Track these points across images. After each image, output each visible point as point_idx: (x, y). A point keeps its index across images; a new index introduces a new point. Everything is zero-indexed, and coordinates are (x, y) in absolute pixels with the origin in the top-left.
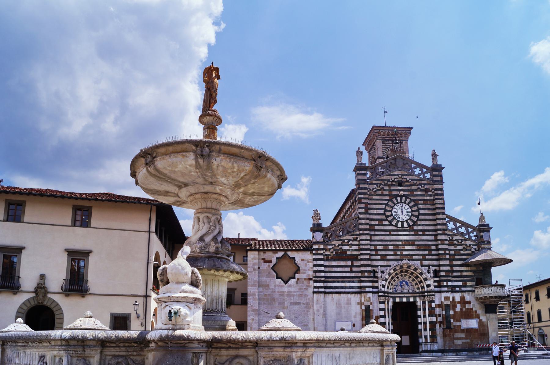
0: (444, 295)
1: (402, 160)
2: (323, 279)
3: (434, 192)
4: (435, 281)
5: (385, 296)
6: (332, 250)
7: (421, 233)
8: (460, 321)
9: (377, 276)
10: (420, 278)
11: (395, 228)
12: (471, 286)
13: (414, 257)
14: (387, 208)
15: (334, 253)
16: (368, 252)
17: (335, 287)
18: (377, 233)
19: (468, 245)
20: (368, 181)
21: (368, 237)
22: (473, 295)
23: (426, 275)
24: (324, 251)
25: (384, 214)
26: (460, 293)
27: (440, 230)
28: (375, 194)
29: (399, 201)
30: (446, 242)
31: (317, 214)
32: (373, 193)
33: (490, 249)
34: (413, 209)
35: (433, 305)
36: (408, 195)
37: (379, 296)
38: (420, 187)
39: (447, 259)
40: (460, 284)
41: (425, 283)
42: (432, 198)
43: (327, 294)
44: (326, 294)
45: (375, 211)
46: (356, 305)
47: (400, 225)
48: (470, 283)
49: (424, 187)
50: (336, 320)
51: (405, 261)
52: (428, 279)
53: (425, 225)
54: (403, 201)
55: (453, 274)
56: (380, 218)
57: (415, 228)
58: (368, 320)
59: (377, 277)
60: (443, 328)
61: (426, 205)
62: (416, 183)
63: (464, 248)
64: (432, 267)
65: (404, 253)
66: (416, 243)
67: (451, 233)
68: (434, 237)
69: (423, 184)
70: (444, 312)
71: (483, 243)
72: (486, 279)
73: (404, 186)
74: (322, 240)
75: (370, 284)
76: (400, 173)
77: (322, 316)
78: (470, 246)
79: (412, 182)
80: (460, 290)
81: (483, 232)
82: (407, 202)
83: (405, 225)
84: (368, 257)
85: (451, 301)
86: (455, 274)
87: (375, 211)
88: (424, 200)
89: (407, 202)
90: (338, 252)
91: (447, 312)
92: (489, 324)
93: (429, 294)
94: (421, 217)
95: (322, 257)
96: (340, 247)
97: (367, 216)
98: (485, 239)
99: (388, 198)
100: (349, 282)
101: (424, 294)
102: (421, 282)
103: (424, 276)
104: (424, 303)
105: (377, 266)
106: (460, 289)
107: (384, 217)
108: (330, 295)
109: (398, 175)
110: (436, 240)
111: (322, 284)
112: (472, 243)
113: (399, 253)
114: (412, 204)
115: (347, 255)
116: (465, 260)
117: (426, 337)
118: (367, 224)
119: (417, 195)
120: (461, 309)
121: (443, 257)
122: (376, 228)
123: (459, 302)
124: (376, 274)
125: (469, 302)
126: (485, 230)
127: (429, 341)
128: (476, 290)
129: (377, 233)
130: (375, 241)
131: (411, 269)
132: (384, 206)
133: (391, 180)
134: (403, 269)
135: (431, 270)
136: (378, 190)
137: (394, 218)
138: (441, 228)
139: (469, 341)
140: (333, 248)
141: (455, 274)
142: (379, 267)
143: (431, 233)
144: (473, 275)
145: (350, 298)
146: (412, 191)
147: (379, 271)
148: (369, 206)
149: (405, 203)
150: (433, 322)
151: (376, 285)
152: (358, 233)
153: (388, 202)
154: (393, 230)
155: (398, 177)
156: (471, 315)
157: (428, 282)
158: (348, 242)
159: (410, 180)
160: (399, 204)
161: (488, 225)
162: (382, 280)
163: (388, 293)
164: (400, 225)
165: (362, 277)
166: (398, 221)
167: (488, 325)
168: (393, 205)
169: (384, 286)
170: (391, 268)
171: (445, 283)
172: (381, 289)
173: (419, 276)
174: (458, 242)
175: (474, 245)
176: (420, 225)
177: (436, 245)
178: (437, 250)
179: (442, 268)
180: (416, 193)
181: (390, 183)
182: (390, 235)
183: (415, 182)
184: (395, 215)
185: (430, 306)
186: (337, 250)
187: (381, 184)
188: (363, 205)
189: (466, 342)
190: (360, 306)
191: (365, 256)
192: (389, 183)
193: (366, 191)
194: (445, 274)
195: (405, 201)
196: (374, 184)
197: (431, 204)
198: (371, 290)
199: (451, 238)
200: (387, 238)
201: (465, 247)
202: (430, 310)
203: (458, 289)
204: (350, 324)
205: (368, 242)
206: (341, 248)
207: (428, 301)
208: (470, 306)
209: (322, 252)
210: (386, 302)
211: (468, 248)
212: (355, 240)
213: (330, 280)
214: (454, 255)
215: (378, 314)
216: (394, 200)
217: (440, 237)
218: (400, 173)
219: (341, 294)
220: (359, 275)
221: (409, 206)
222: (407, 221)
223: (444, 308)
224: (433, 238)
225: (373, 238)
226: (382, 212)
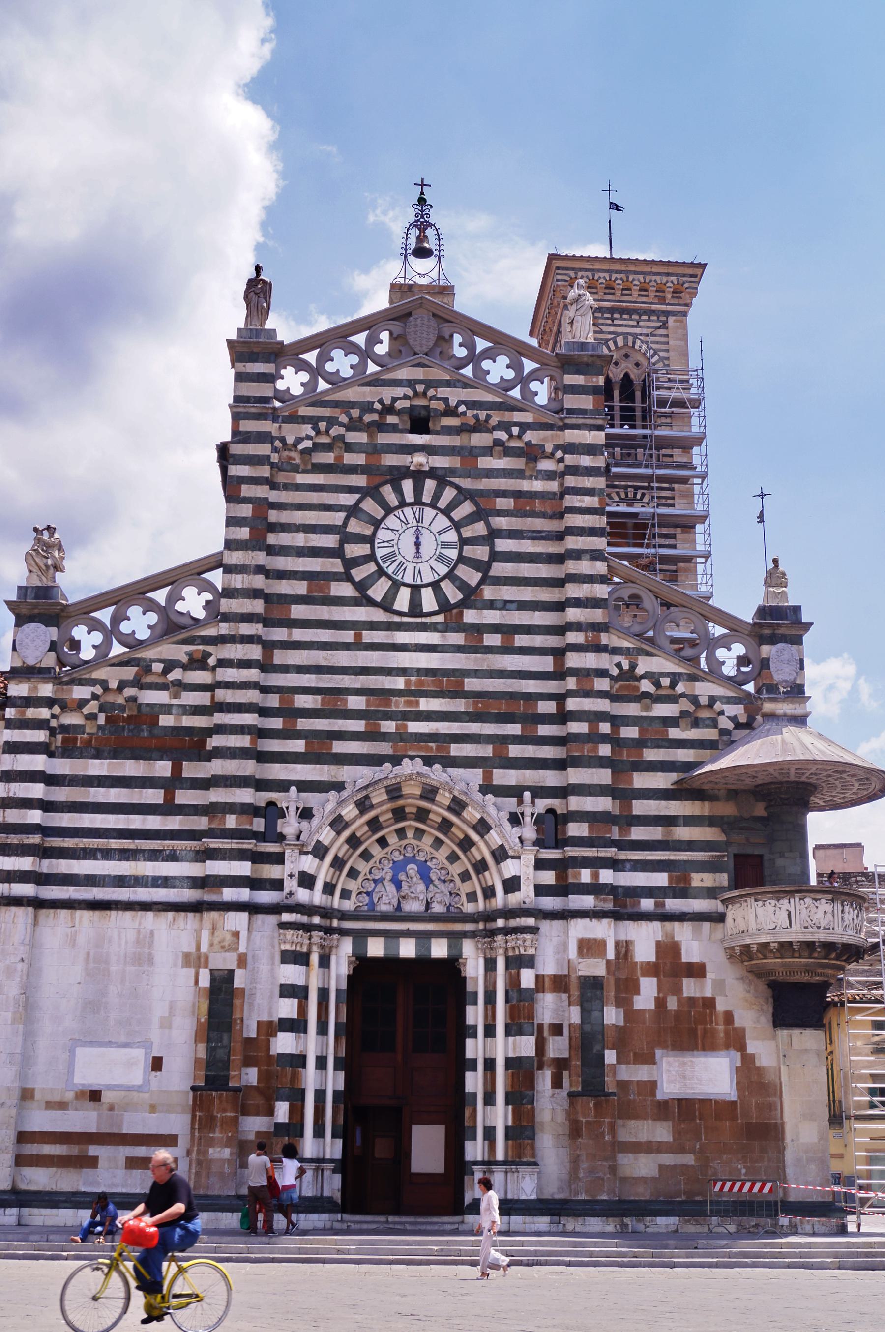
0: (580, 929)
1: (433, 322)
2: (35, 839)
3: (562, 460)
4: (540, 864)
5: (308, 928)
6: (92, 707)
7: (492, 640)
8: (654, 1063)
9: (281, 833)
10: (479, 849)
11: (379, 615)
12: (711, 893)
13: (456, 750)
14: (355, 526)
15: (102, 719)
16: (249, 719)
17: (85, 875)
18: (298, 635)
19: (704, 701)
20: (275, 409)
21: (255, 652)
22: (719, 935)
23: (501, 833)
24: (57, 710)
25: (337, 553)
26: (657, 925)
27: (576, 626)
28: (304, 462)
29: (409, 497)
30: (602, 684)
31: (48, 547)
32: (298, 461)
33: (800, 720)
34: (467, 533)
35: (527, 979)
36: (452, 471)
37: (283, 926)
38: (502, 435)
39: (602, 762)
40: (661, 879)
41: (500, 872)
42: (553, 486)
43: (52, 911)
44: (43, 912)
45: (300, 540)
46: (175, 965)
47: (403, 601)
48: (705, 876)
49: (519, 437)
50: (76, 1037)
51: (408, 767)
52: (511, 853)
53: (514, 606)
54: (426, 498)
55: (629, 832)
56: (318, 569)
57: (470, 616)
58: (221, 1040)
59: (281, 838)
60: (571, 1095)
61: (525, 515)
62: (486, 421)
63: (684, 714)
64: (533, 797)
65: (414, 727)
66: (472, 684)
67: (626, 644)
68: (550, 659)
69: (516, 424)
70: (575, 1015)
71: (768, 692)
72: (780, 862)
73: (437, 433)
74: (50, 660)
75: (243, 868)
76: (419, 373)
77: (9, 1015)
78: (710, 705)
79: (470, 413)
80: (660, 910)
81: (773, 640)
82: (443, 503)
83: (429, 601)
84: (243, 741)
85: (608, 962)
86: (638, 833)
87: (300, 540)
88: (517, 495)
89: (443, 503)
90: (118, 716)
91: (590, 1012)
92: (784, 1078)
93: (514, 923)
94: (499, 569)
95: (40, 736)
96: (129, 692)
97: (260, 558)
98: (780, 673)
99: (360, 481)
100: (154, 855)
101: (491, 926)
102: (481, 867)
103: (495, 838)
104: (490, 965)
105: (283, 786)
106: (656, 904)
107: (335, 565)
108: (63, 913)
109: (411, 383)
110: (560, 674)
111: (25, 863)
112: (718, 690)
113: (388, 726)
114: (466, 509)
115: (156, 731)
116: (689, 766)
117: (489, 1133)
118: (256, 594)
119: (490, 473)
120: (660, 1002)
121: (586, 750)
122: (298, 611)
123: (652, 970)
124: (280, 821)
125: (697, 971)
126: (782, 631)
127: (500, 1156)
128: (732, 913)
129: (298, 635)
130: (285, 669)
131: (440, 805)
132: (343, 515)
133: (377, 406)
134: (401, 803)
135: (528, 811)
136: (317, 447)
137: (381, 572)
138: (582, 619)
139: (689, 1159)
140: (95, 697)
141: (638, 833)
142: (293, 789)
143: (538, 641)
144: (722, 838)
145: (152, 933)
146: (470, 454)
147: (292, 809)
148: (274, 516)
149: (433, 505)
150: (519, 1059)
151: (272, 871)
152: (211, 632)
153: (359, 501)
154: (373, 626)
155: (410, 393)
156: (705, 1031)
157: (510, 868)
158: (166, 671)
159: (462, 408)
160: (408, 511)
161: (797, 609)
162: (302, 853)
163: (326, 913)
164: (403, 601)
165: (210, 833)
166: (396, 585)
167: (781, 1083)
168: (379, 513)
169: (307, 880)
170: (345, 794)
171: (586, 876)
172: (291, 894)
173: (475, 837)
174: (658, 685)
175: (729, 700)
176: (491, 605)
177: (560, 698)
178: (563, 717)
179: (575, 803)
180: (485, 462)
181: (375, 417)
182: (358, 646)
183: (482, 414)
184: (385, 558)
185: (513, 982)
186: (113, 705)
187: (332, 421)
188: (246, 511)
189: (675, 1166)
190: (192, 971)
191: (233, 737)
192: (368, 418)
193: (263, 449)
194: (591, 829)
195: (437, 496)
196: (305, 420)
197: (549, 512)
198: (244, 894)
199: (626, 666)
200: (343, 658)
201: (691, 708)
202: (514, 1002)
203: (647, 904)
204: (139, 1057)
205: (252, 674)
206: (134, 699)
207: (508, 960)
208: (702, 988)
209: (44, 713)
210: (315, 958)
211: (705, 714)
212: (198, 663)
213: (69, 843)
214: (640, 743)
215: (270, 1014)
216: (388, 492)
217: (573, 660)
218: (419, 373)
219: (113, 913)
220: (201, 823)
221: (451, 519)
222: (435, 585)
223: (575, 993)
224: (546, 663)
225: (280, 657)
226: (329, 541)
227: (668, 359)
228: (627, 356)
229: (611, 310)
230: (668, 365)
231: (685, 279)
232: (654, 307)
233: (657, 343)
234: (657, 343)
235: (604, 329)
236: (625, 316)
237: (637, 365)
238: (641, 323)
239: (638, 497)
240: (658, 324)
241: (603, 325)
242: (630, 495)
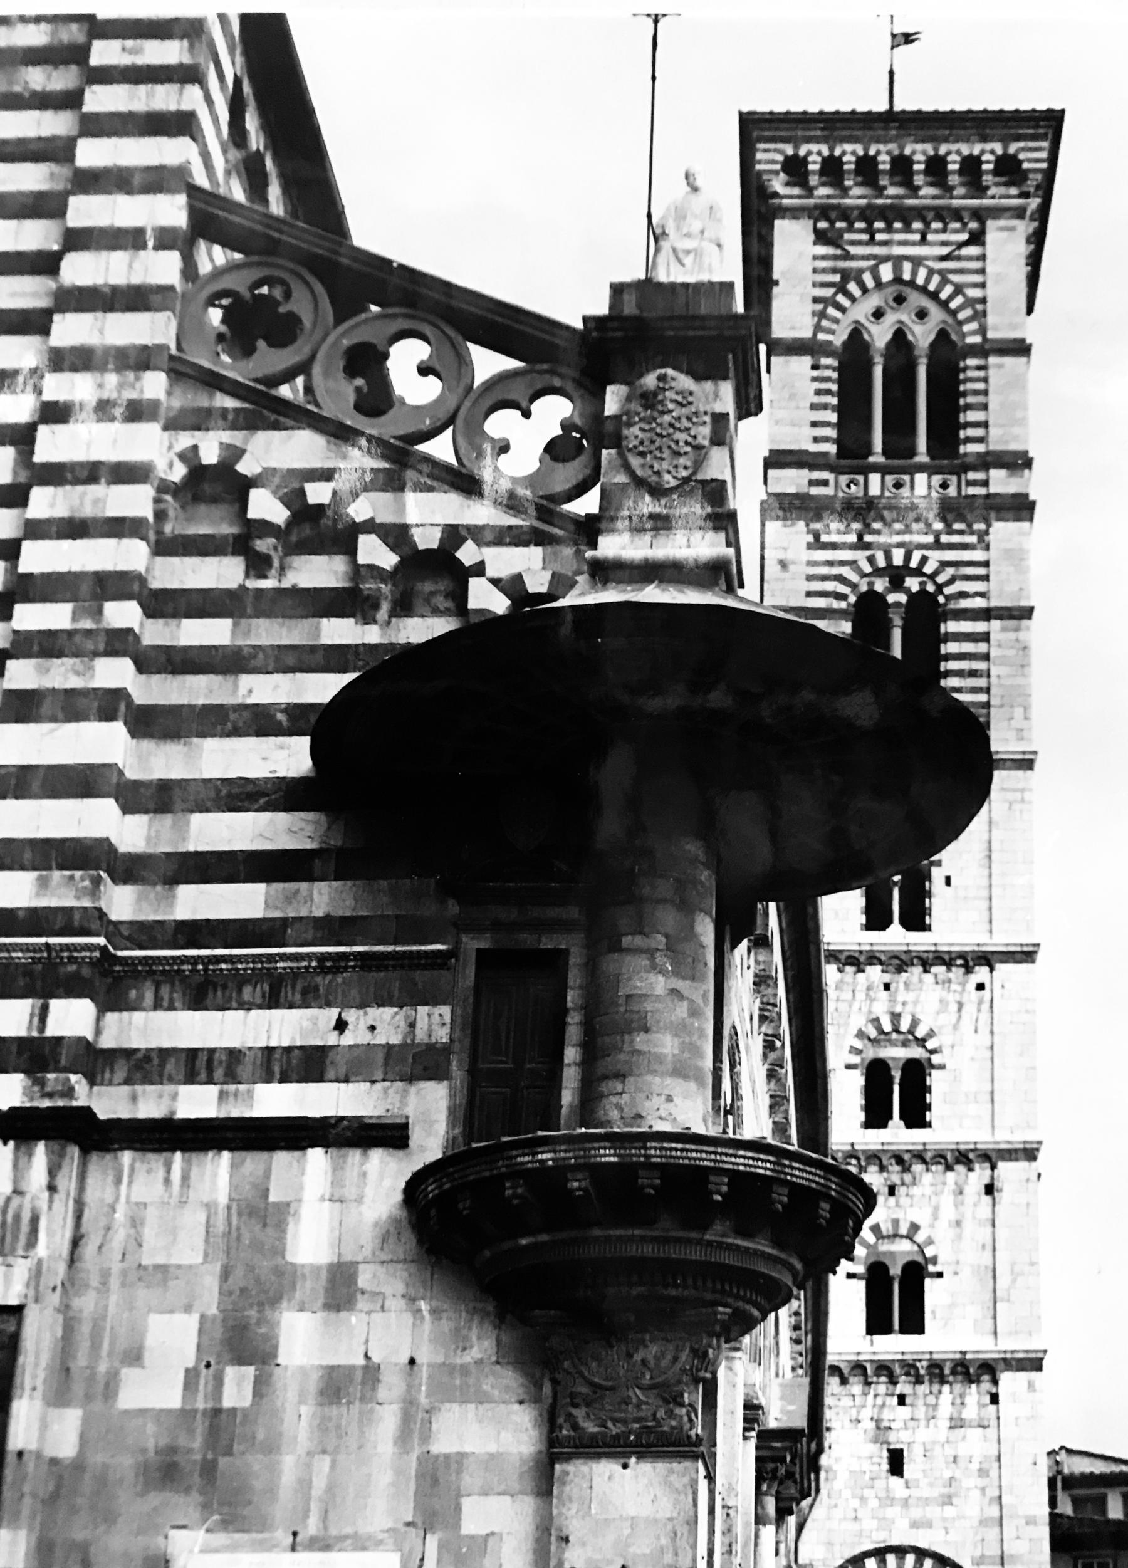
227: (984, 300)
228: (900, 300)
229: (868, 214)
230: (984, 314)
231: (1022, 144)
232: (956, 202)
233: (961, 271)
234: (961, 271)
235: (853, 250)
236: (898, 225)
237: (922, 314)
238: (930, 237)
239: (914, 564)
240: (965, 236)
241: (853, 243)
242: (898, 558)
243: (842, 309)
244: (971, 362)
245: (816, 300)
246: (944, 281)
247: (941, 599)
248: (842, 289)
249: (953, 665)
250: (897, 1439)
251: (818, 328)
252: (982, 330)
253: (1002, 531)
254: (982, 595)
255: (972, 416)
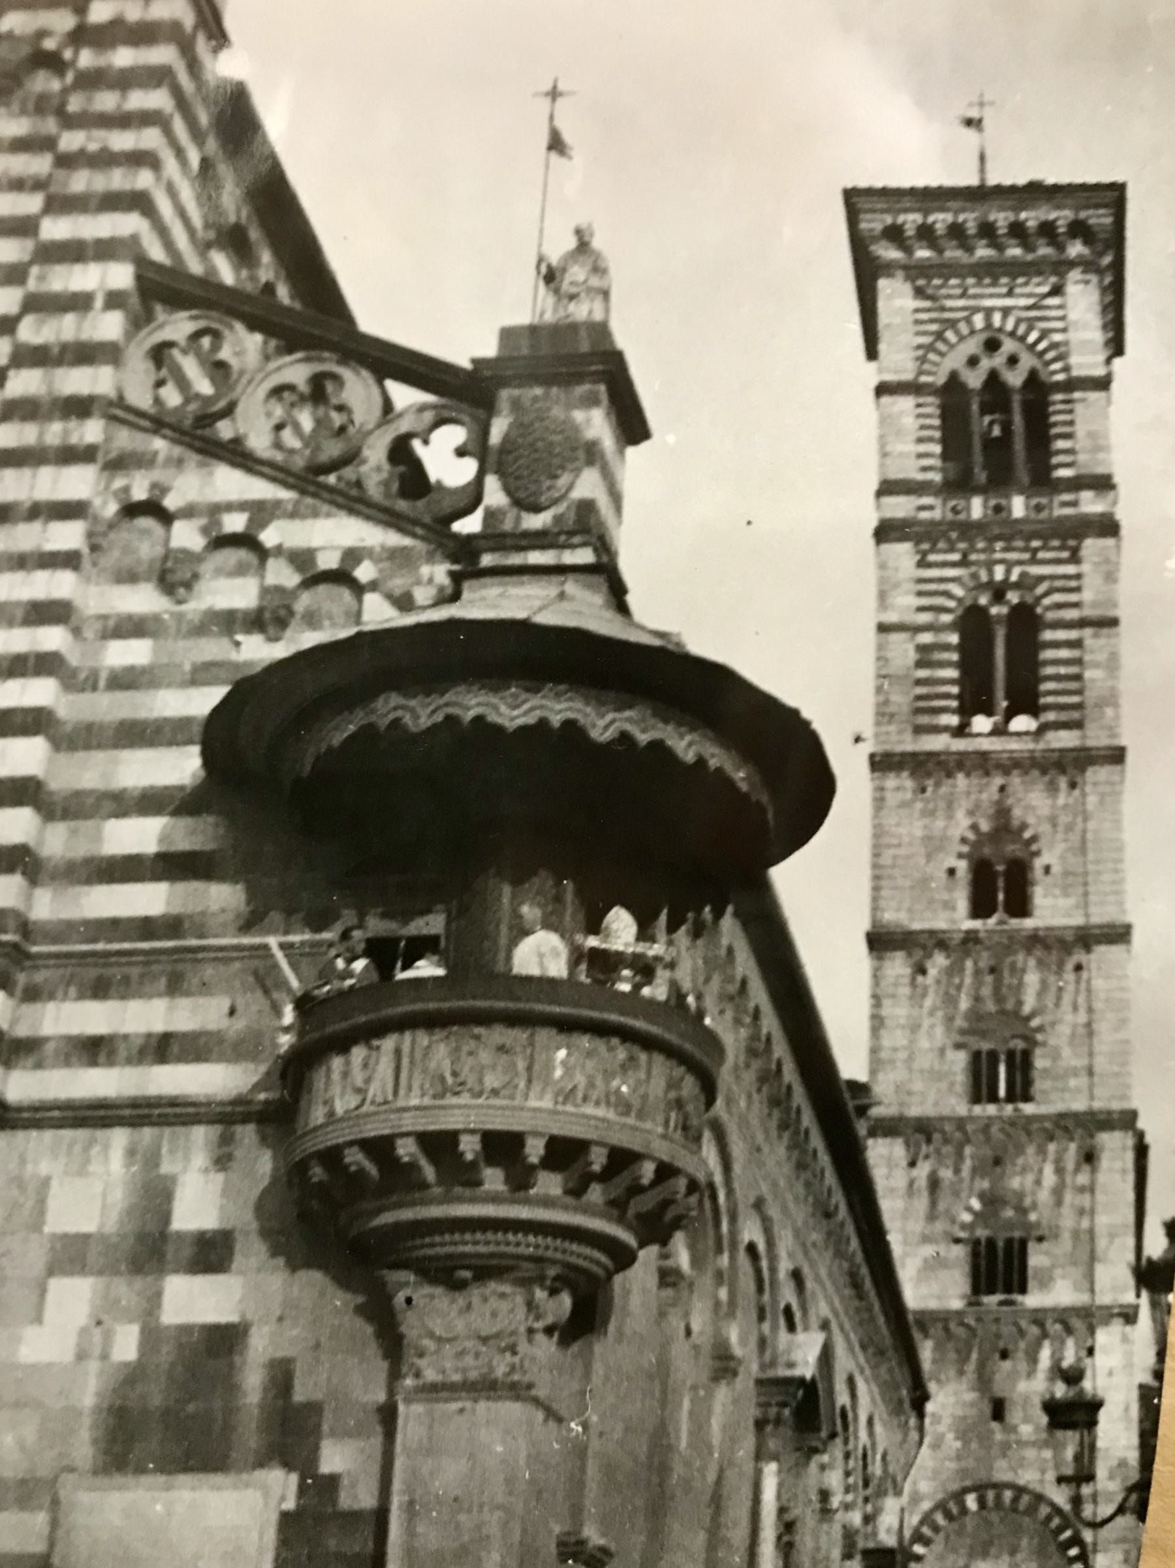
235: (949, 303)
238: (1018, 290)
240: (1045, 289)
243: (942, 354)
244: (1059, 397)
245: (919, 347)
246: (1030, 329)
247: (1039, 610)
248: (939, 336)
249: (1049, 670)
250: (999, 1389)
251: (921, 373)
252: (1066, 369)
253: (1091, 546)
254: (1076, 605)
255: (1061, 444)
